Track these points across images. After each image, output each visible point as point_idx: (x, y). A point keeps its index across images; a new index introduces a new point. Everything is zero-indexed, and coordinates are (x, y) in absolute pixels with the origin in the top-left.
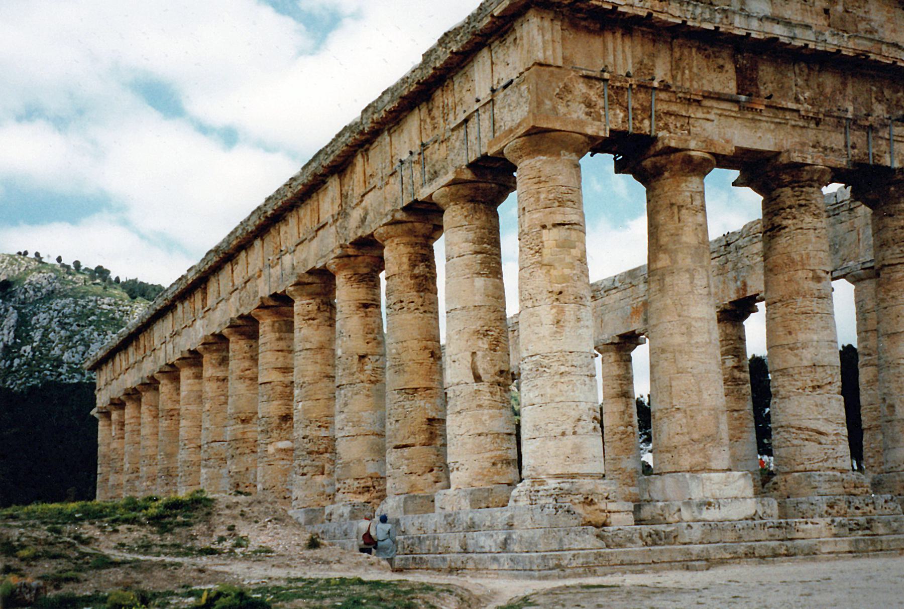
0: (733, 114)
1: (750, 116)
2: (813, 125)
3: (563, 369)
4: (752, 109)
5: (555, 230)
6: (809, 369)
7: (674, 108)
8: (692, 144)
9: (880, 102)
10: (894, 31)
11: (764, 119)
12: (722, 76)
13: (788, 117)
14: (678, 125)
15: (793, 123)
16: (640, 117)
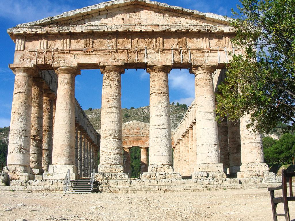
0: (81, 54)
1: (88, 54)
2: (113, 53)
3: (12, 134)
4: (88, 52)
5: (16, 94)
6: (104, 131)
7: (59, 55)
8: (62, 65)
9: (143, 43)
10: (151, 20)
11: (94, 54)
12: (80, 44)
13: (103, 52)
14: (61, 60)
15: (105, 53)
16: (47, 60)
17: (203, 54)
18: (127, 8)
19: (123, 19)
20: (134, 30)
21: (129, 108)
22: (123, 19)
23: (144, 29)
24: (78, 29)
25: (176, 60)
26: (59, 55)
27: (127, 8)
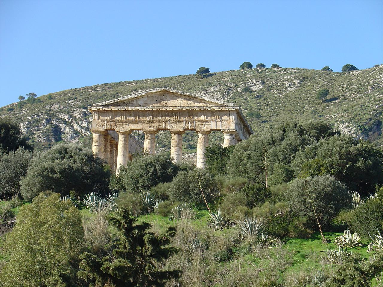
7: (119, 124)
17: (202, 123)
18: (159, 93)
19: (157, 100)
20: (162, 109)
21: (337, 68)
22: (157, 100)
23: (168, 109)
24: (130, 108)
25: (186, 127)
26: (119, 124)
27: (159, 93)
